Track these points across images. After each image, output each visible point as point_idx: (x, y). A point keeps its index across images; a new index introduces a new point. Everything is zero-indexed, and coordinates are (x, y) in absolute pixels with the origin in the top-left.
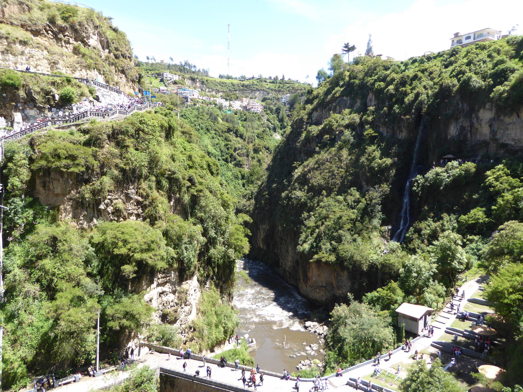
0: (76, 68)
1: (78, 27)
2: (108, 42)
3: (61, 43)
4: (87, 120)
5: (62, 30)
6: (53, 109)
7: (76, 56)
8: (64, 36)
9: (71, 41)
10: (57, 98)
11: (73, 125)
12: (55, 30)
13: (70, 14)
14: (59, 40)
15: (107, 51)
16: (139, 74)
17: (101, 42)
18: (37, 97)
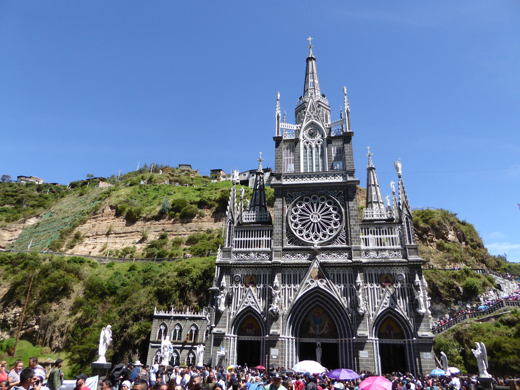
0: (445, 263)
1: (438, 226)
2: (463, 234)
3: (427, 243)
4: (505, 311)
5: (425, 231)
6: (459, 302)
7: (442, 253)
8: (428, 236)
9: (435, 239)
10: (461, 289)
11: (492, 317)
12: (420, 232)
13: (429, 216)
14: (424, 240)
15: (464, 243)
16: (497, 262)
17: (458, 236)
18: (442, 291)
